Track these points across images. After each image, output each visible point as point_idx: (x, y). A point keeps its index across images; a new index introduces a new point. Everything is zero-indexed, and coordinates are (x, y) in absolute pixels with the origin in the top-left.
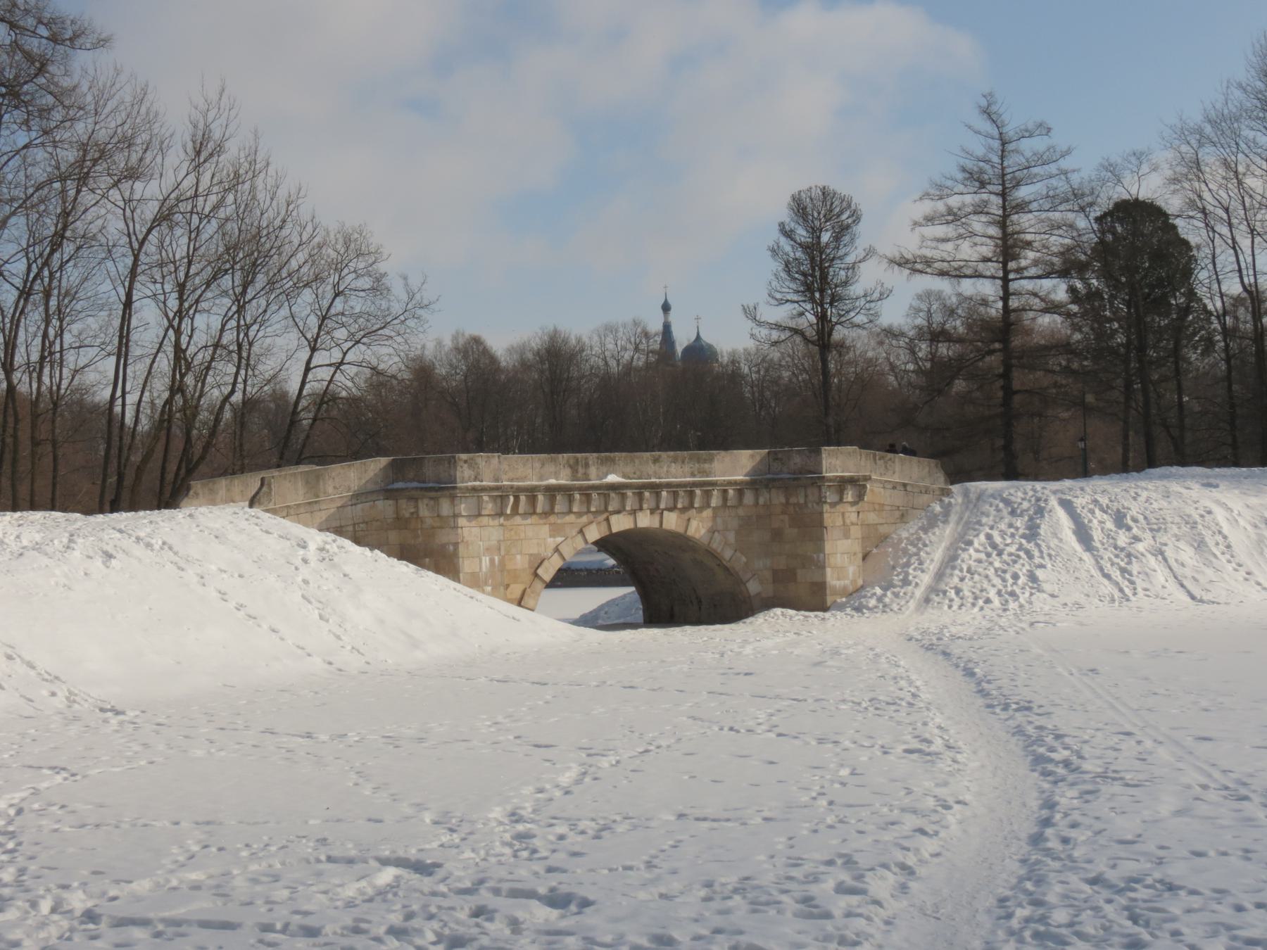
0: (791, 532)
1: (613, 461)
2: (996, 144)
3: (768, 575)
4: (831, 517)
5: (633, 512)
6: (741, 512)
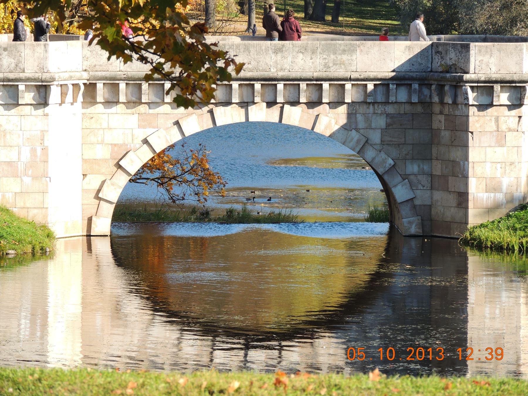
4: (477, 120)
5: (245, 104)
6: (390, 109)
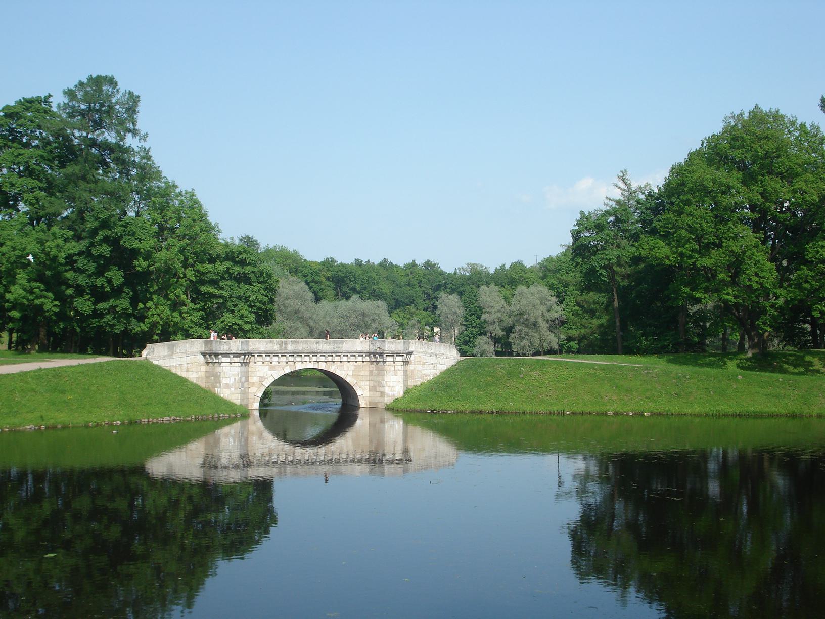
0: (375, 372)
1: (298, 342)
2: (627, 193)
3: (368, 388)
4: (388, 367)
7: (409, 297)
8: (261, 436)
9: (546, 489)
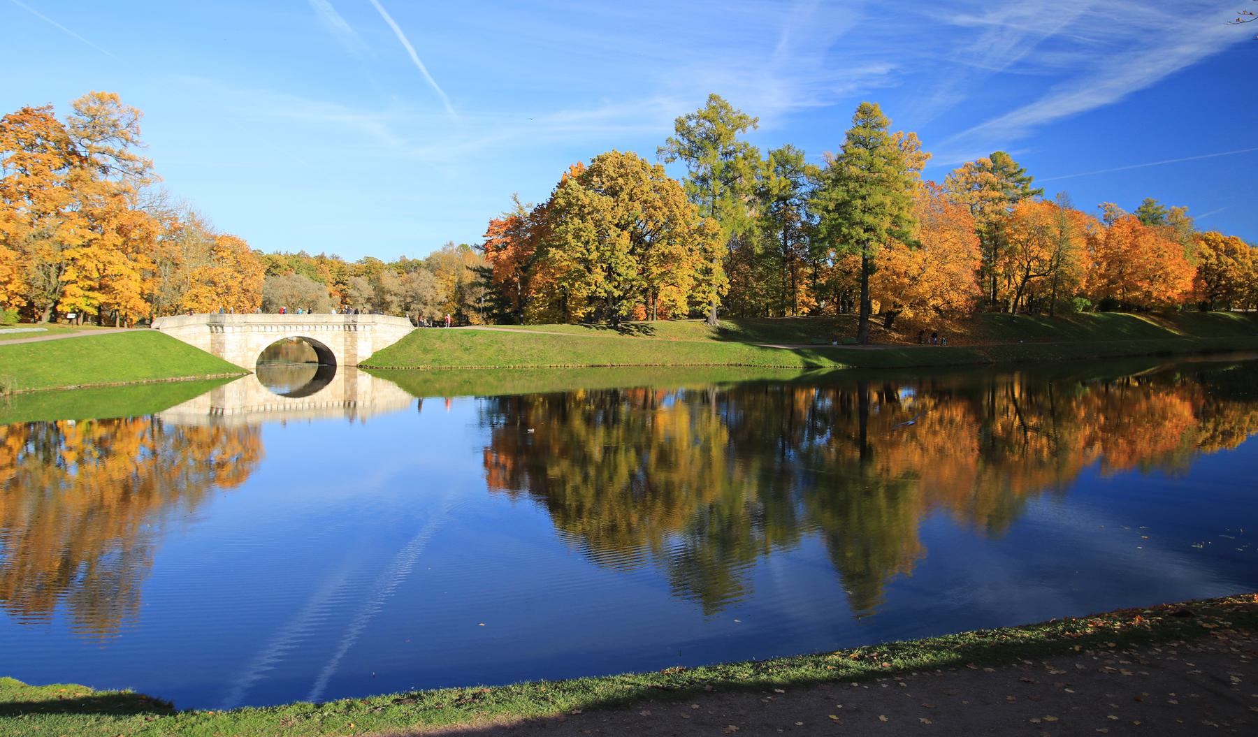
7: (361, 289)
8: (258, 391)
9: (456, 433)
